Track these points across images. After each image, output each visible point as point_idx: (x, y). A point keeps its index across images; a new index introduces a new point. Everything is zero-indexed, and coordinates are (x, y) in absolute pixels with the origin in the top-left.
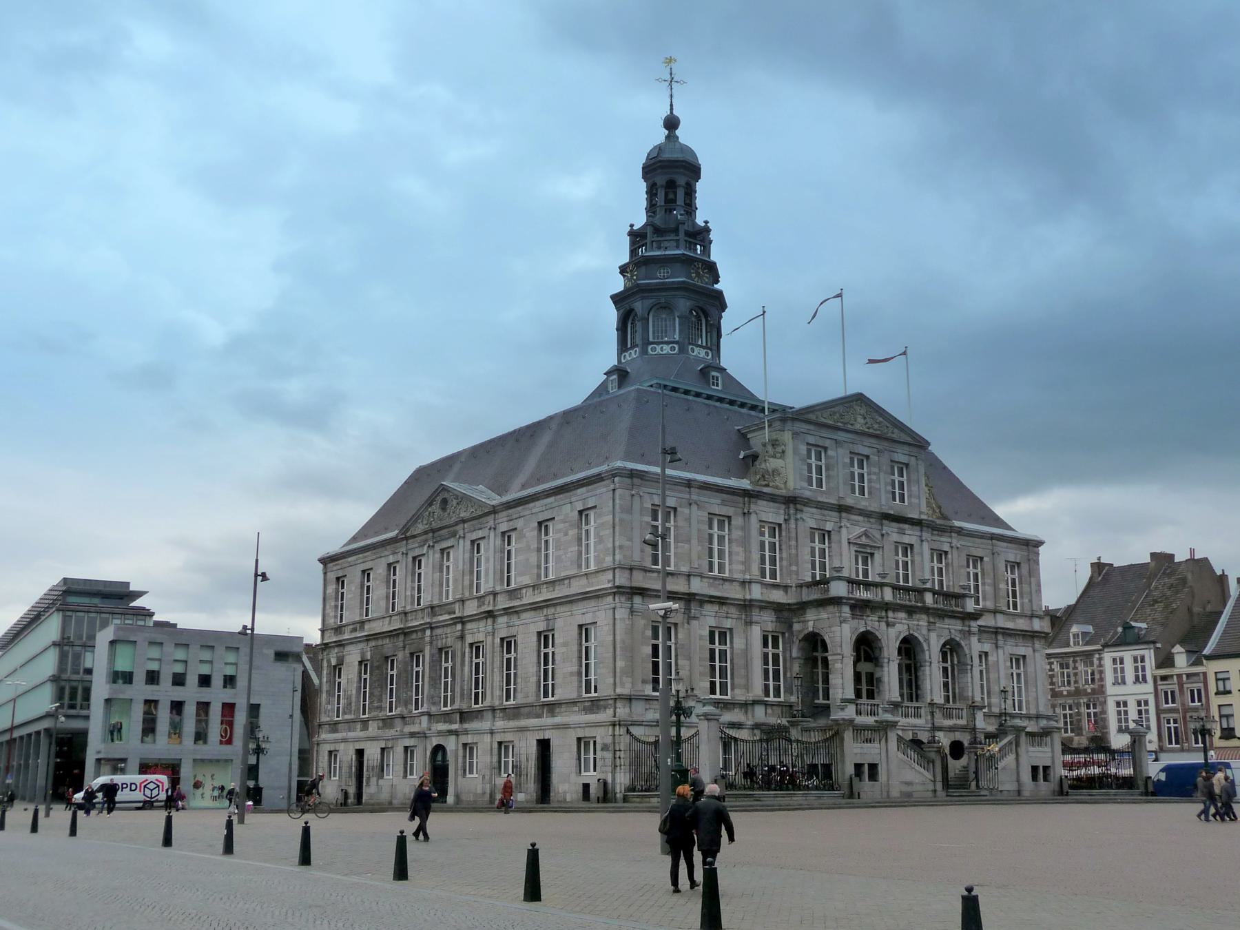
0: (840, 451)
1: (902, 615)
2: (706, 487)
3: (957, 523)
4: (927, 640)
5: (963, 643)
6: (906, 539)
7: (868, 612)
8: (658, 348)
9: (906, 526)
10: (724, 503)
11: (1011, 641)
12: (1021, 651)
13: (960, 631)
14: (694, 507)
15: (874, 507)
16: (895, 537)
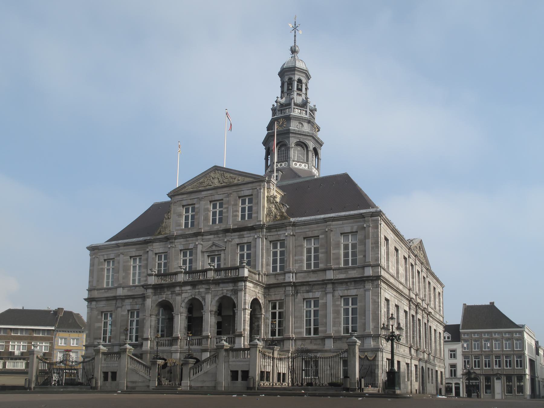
0: (203, 203)
1: (189, 288)
2: (126, 245)
3: (292, 220)
4: (204, 299)
5: (233, 297)
6: (245, 240)
7: (166, 290)
8: (298, 164)
9: (246, 232)
10: (137, 250)
11: (344, 286)
12: (353, 292)
13: (232, 290)
14: (121, 256)
15: (223, 226)
16: (237, 241)
